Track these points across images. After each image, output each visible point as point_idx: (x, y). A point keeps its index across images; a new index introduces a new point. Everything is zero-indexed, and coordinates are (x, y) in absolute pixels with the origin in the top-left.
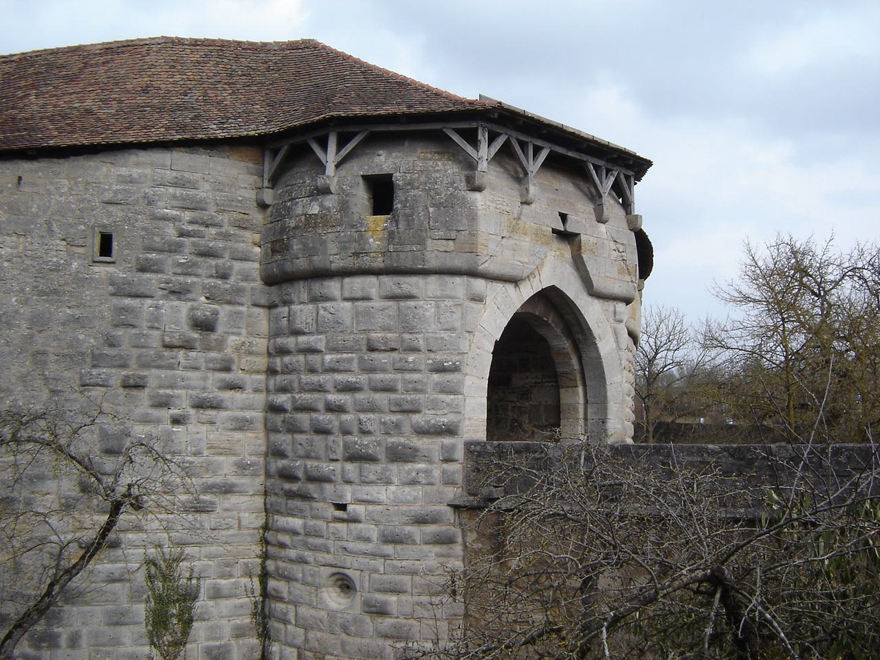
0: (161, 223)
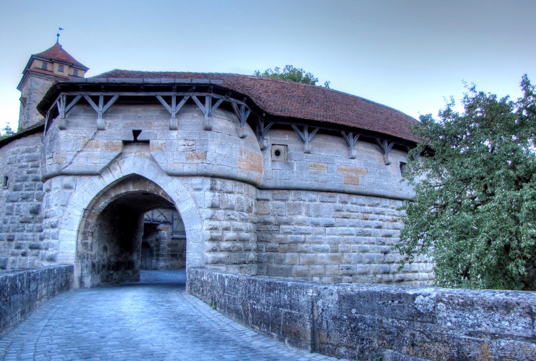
0: (21, 169)
